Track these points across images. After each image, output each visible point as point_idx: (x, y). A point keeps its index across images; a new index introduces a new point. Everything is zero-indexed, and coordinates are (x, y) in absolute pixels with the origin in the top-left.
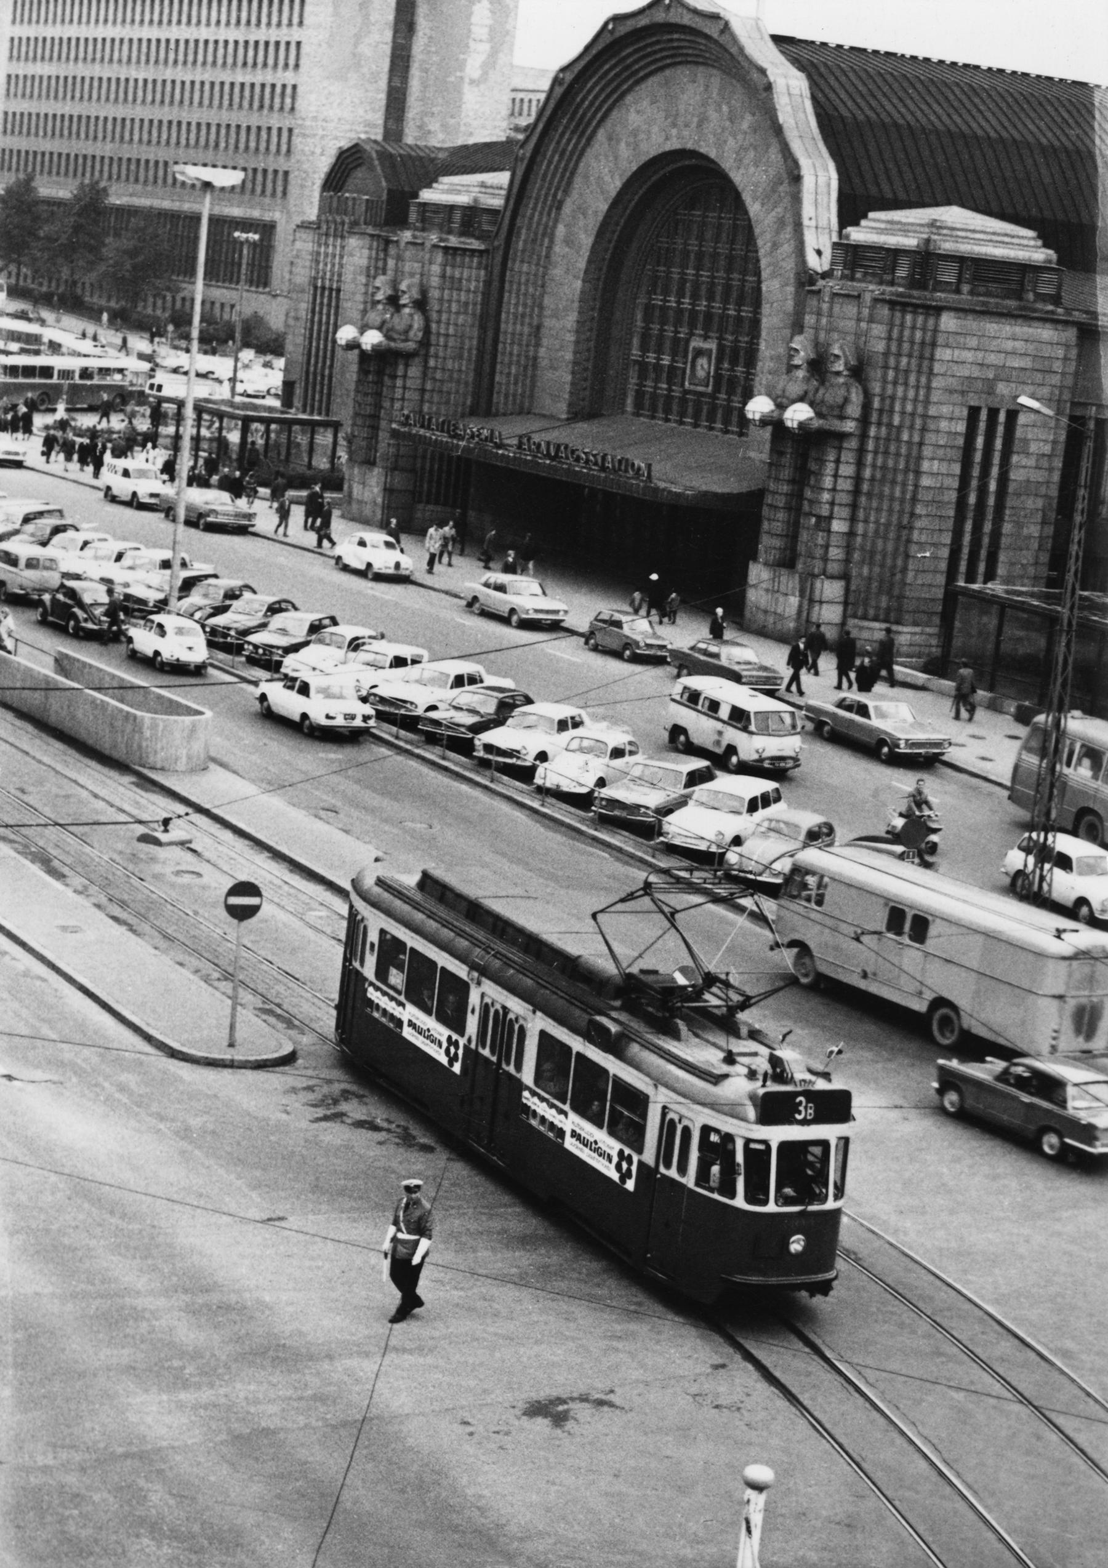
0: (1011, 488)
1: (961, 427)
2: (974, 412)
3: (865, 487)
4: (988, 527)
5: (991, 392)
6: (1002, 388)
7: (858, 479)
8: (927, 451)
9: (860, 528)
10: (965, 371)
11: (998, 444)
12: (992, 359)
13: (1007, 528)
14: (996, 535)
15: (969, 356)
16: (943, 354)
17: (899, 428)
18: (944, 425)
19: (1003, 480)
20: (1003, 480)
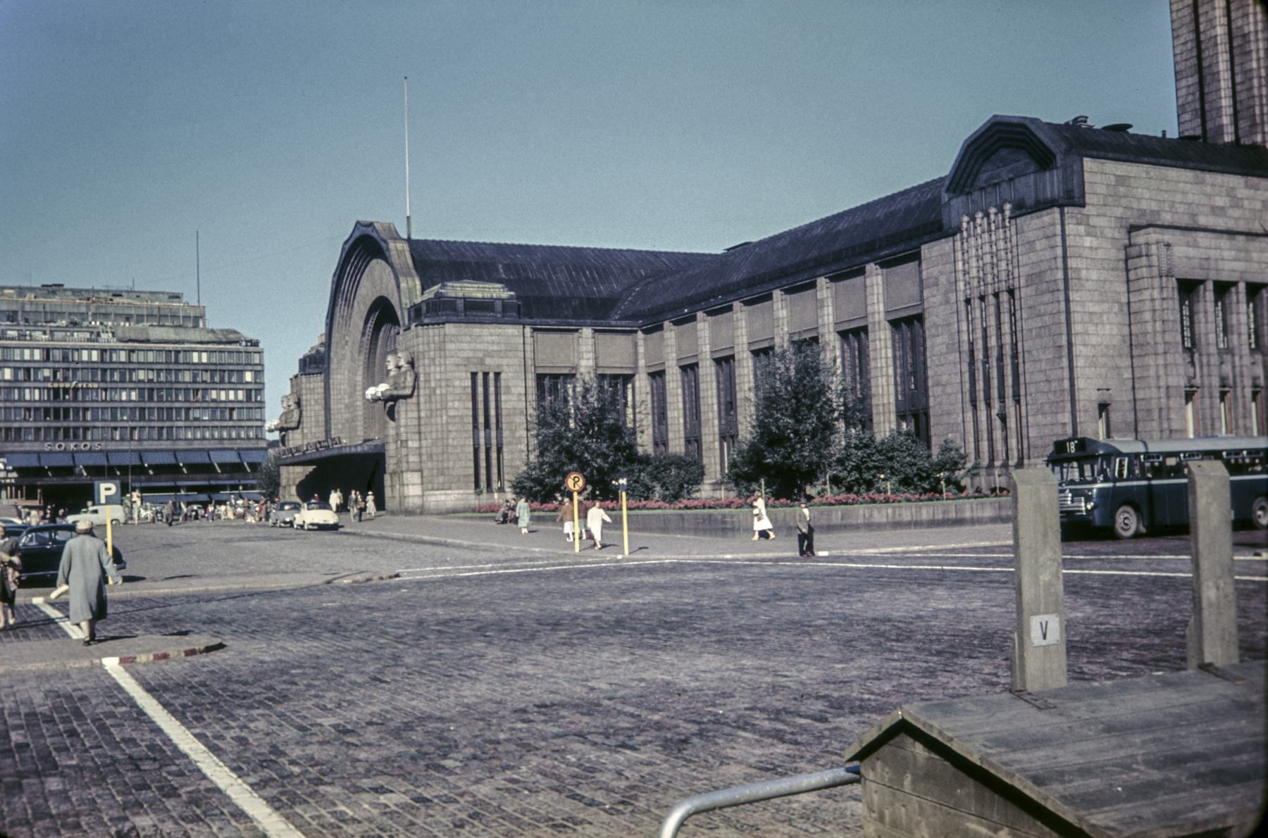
0: (504, 413)
1: (469, 383)
2: (474, 375)
3: (423, 422)
4: (493, 434)
5: (482, 362)
6: (488, 361)
7: (419, 418)
8: (450, 398)
9: (424, 443)
10: (466, 354)
11: (492, 389)
12: (479, 346)
13: (505, 434)
14: (499, 437)
15: (465, 346)
16: (450, 346)
17: (434, 389)
18: (457, 383)
19: (497, 408)
20: (497, 408)
